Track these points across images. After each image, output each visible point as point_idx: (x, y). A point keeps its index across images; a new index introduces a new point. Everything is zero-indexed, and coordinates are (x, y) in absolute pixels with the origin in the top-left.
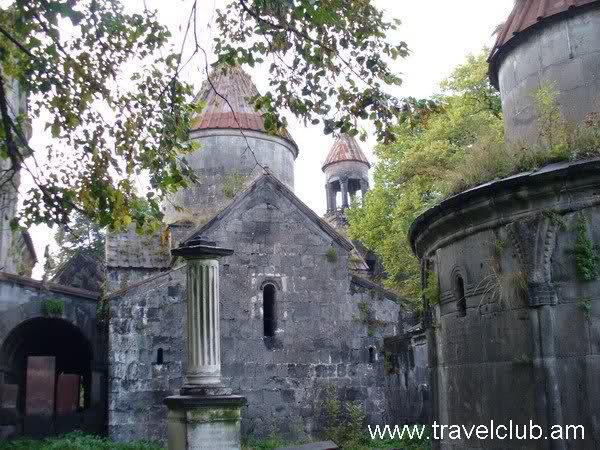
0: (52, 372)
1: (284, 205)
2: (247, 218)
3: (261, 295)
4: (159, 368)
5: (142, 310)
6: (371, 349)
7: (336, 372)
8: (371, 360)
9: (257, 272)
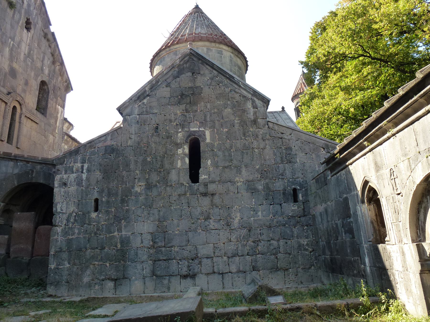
1: (207, 72)
2: (174, 85)
5: (82, 167)
6: (295, 190)
7: (260, 213)
8: (296, 200)
9: (183, 128)
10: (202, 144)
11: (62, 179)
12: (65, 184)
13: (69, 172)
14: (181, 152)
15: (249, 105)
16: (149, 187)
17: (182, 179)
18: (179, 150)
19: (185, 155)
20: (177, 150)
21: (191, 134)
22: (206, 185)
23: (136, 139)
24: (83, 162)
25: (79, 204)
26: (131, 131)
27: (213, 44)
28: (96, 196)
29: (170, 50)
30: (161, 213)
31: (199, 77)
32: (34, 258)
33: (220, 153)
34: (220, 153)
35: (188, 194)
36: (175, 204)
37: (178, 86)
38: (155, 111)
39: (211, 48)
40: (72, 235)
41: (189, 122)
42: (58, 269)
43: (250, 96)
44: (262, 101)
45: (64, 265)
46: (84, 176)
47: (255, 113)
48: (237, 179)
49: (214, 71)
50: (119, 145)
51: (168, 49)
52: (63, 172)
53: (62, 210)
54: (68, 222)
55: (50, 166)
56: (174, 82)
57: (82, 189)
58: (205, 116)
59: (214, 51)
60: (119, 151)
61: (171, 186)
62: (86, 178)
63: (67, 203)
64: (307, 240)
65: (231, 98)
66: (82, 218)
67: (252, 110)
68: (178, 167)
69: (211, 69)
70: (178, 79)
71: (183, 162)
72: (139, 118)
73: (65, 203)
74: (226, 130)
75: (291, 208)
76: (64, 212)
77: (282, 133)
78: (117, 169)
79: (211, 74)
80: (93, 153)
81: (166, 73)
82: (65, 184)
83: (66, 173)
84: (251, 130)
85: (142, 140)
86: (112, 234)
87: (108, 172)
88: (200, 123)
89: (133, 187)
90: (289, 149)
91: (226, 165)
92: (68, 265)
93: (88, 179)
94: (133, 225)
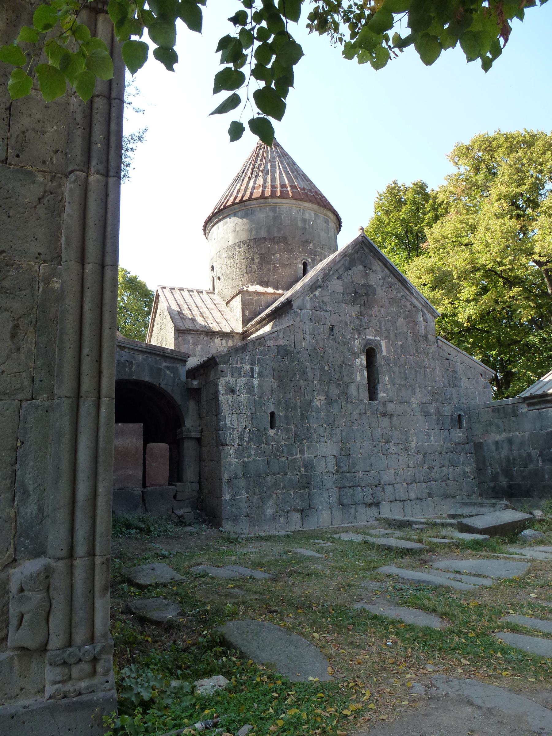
0: (140, 442)
3: (364, 358)
4: (272, 432)
5: (252, 369)
6: (460, 416)
7: (432, 438)
9: (359, 334)
10: (378, 356)
11: (227, 383)
12: (233, 391)
13: (235, 375)
14: (359, 363)
15: (420, 318)
16: (329, 401)
17: (361, 395)
18: (357, 360)
19: (363, 367)
20: (355, 360)
21: (368, 342)
22: (385, 405)
23: (311, 341)
24: (253, 363)
25: (252, 418)
26: (304, 329)
27: (321, 209)
28: (272, 408)
29: (266, 203)
30: (344, 434)
31: (371, 274)
32: (149, 489)
33: (396, 369)
34: (396, 369)
35: (369, 413)
36: (356, 424)
37: (351, 281)
38: (329, 308)
39: (319, 214)
40: (248, 458)
41: (365, 327)
42: (234, 500)
43: (420, 307)
44: (432, 315)
45: (242, 494)
46: (256, 382)
47: (426, 328)
48: (412, 400)
49: (386, 269)
50: (293, 345)
51: (262, 201)
52: (229, 375)
53: (232, 425)
54: (241, 441)
55: (158, 358)
56: (345, 274)
57: (255, 399)
58: (380, 323)
59: (321, 218)
60: (293, 353)
61: (351, 402)
62: (258, 384)
63: (238, 416)
64: (470, 467)
65: (404, 306)
66: (258, 436)
67: (423, 324)
68: (358, 380)
69: (383, 267)
70: (350, 272)
71: (361, 376)
72: (313, 314)
73: (235, 415)
74: (400, 343)
75: (458, 435)
76: (235, 427)
77: (449, 354)
78: (292, 377)
79: (383, 272)
80: (263, 353)
81: (339, 262)
82: (233, 391)
83: (232, 376)
84: (422, 345)
85: (317, 343)
86: (295, 457)
87: (284, 379)
88: (375, 330)
89: (312, 400)
90: (455, 372)
91: (402, 383)
92: (246, 495)
93: (261, 386)
94: (316, 446)
